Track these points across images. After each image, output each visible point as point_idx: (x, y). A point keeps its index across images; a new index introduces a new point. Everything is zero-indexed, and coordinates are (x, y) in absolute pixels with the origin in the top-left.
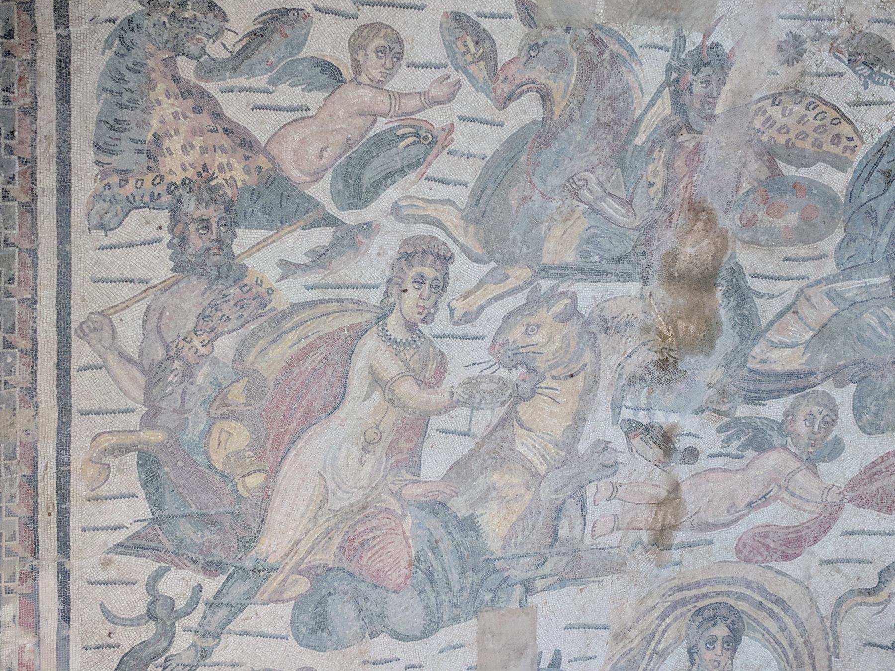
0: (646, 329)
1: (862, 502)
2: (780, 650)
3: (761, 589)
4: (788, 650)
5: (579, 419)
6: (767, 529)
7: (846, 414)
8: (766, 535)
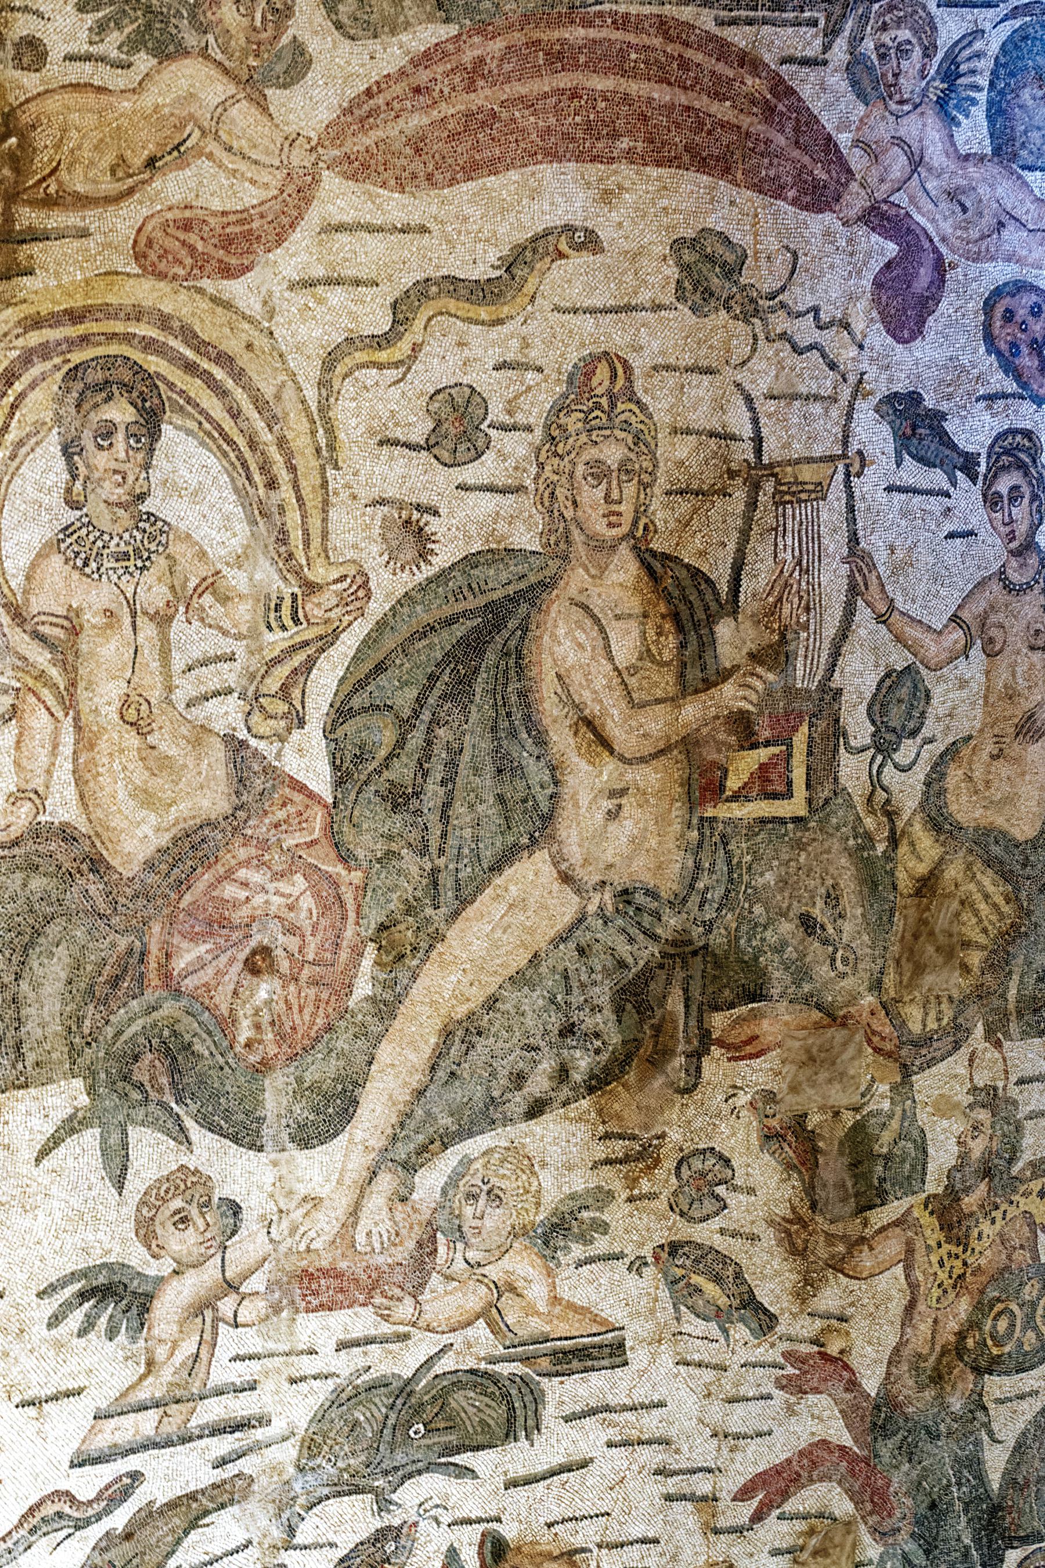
2: (232, 455)
3: (188, 335)
4: (248, 454)
6: (188, 214)
8: (187, 226)
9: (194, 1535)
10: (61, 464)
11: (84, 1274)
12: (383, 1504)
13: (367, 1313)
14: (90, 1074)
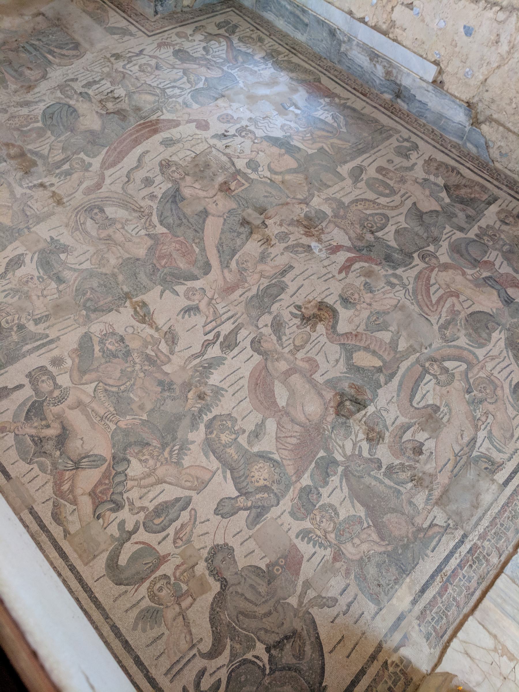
0: (16, 169)
1: (107, 168)
5: (12, 192)
7: (85, 158)
9: (238, 335)
10: (91, 220)
11: (183, 309)
12: (270, 313)
13: (240, 289)
14: (160, 284)
